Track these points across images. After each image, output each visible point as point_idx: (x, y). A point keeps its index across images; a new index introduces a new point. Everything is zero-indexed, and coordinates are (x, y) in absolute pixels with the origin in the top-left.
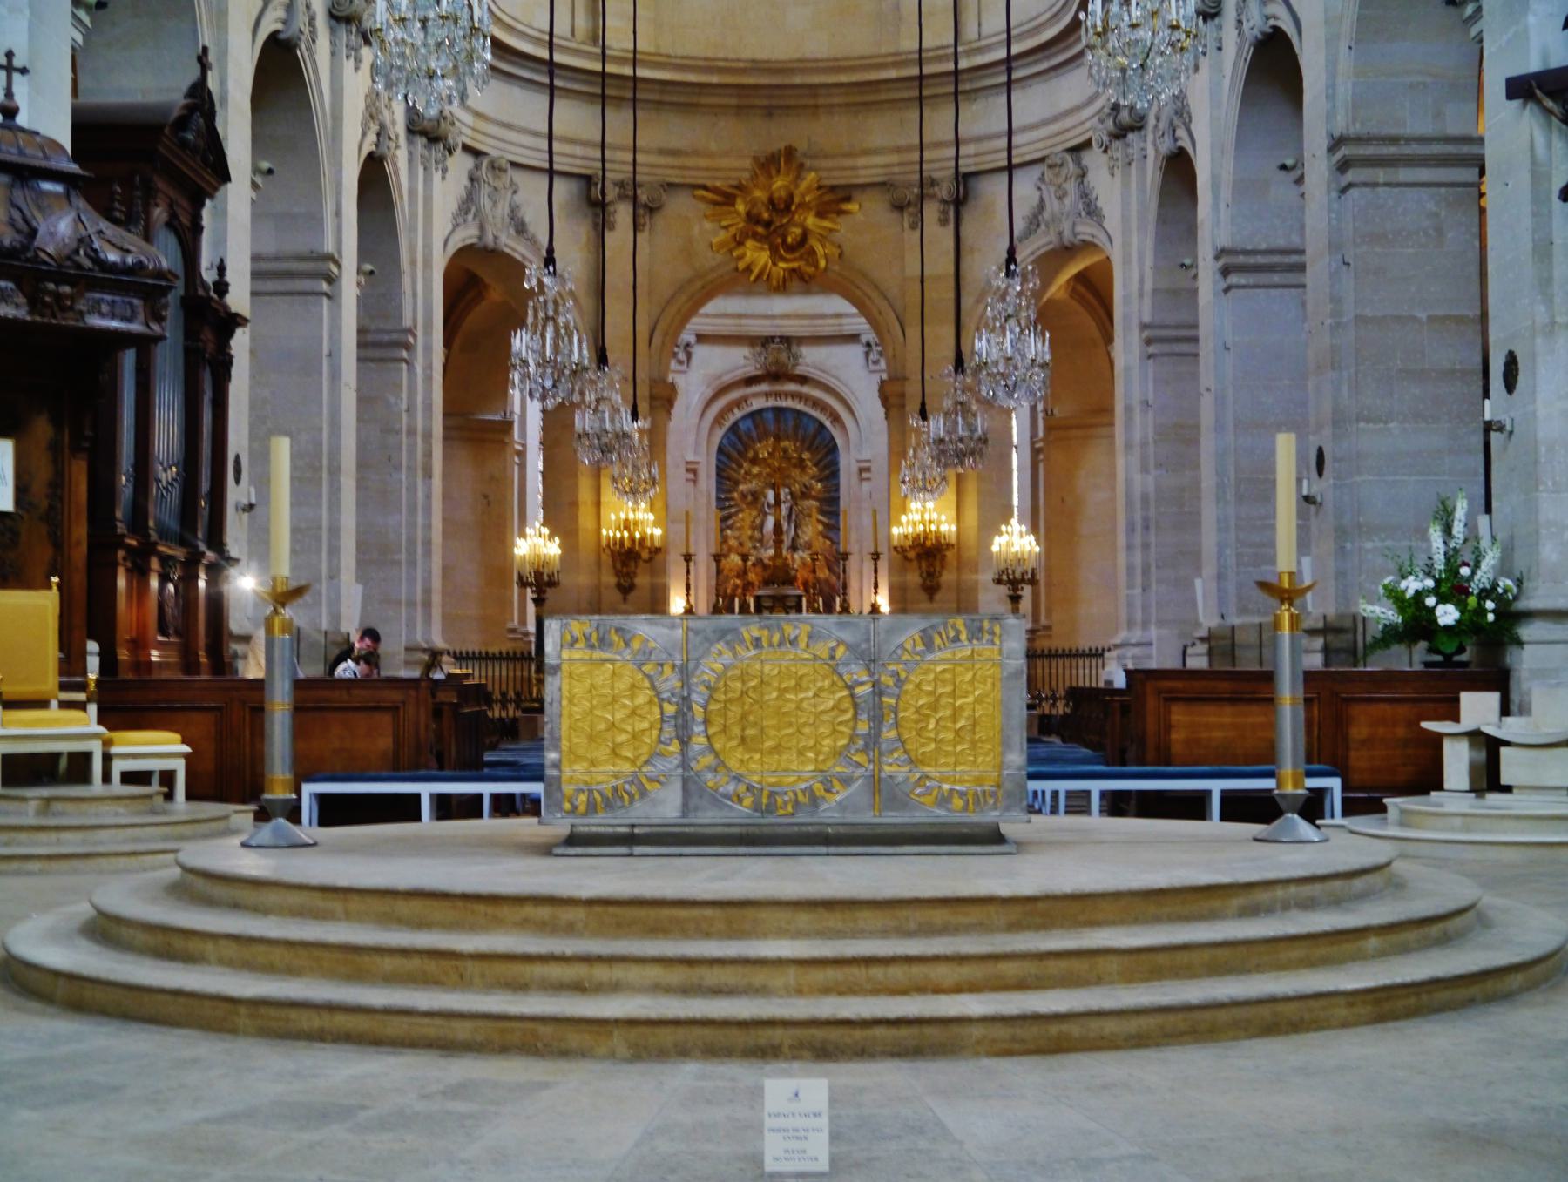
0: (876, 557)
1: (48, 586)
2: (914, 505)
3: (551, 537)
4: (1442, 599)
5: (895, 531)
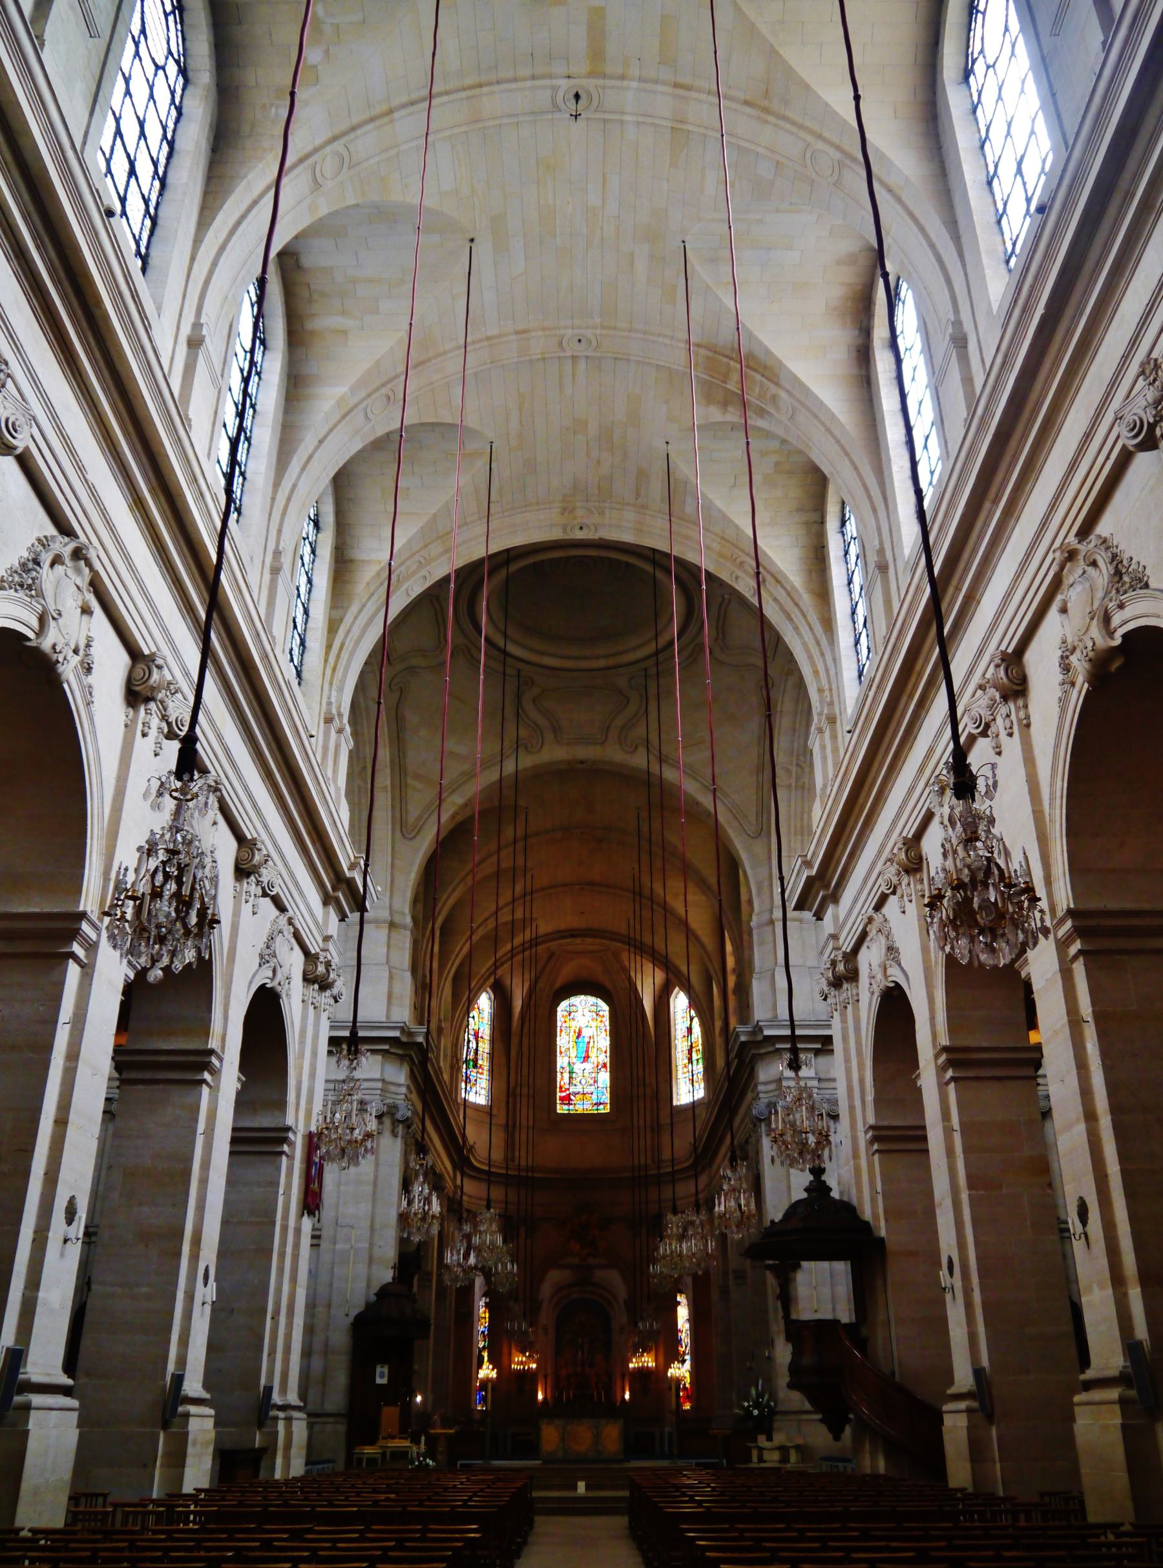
0: (623, 1376)
1: (396, 1405)
2: (634, 1360)
3: (493, 1369)
4: (754, 1409)
5: (631, 1365)
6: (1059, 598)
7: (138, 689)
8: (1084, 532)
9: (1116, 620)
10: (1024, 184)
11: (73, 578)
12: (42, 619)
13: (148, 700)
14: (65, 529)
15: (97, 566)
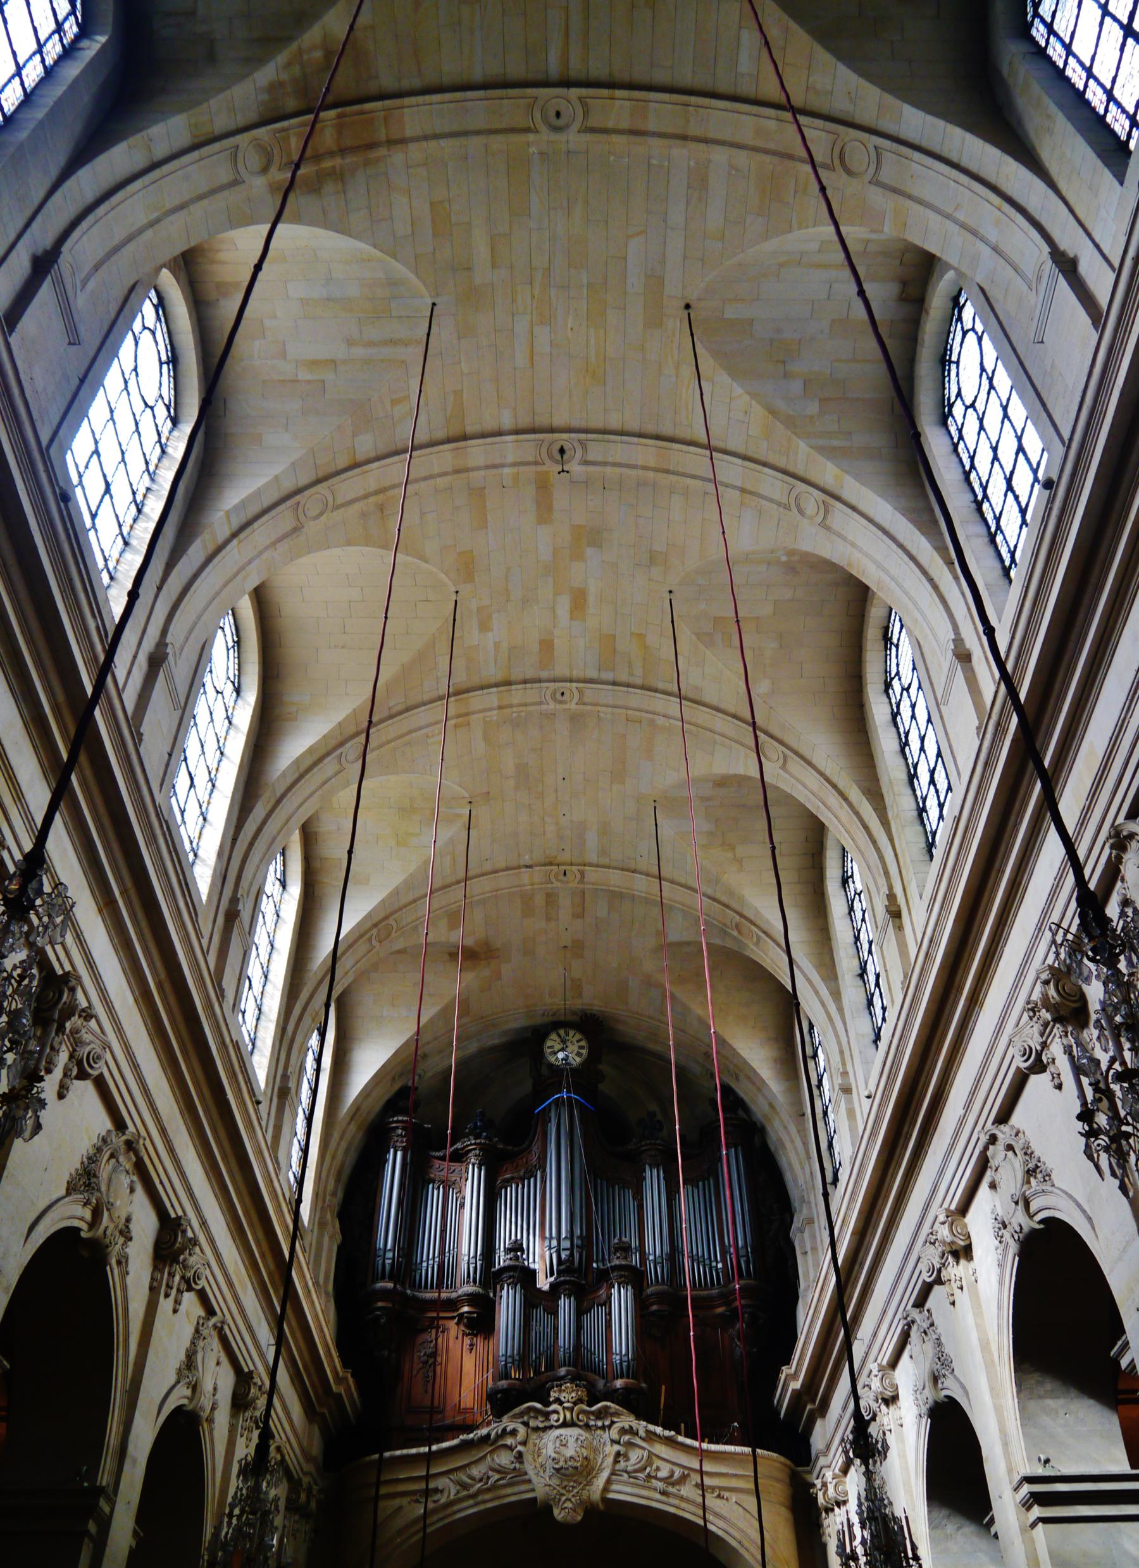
6: (988, 1176)
7: (165, 1252)
8: (1003, 1117)
9: (1033, 1207)
10: (937, 791)
11: (124, 1164)
12: (97, 1214)
13: (175, 1260)
14: (120, 1125)
15: (143, 1153)
